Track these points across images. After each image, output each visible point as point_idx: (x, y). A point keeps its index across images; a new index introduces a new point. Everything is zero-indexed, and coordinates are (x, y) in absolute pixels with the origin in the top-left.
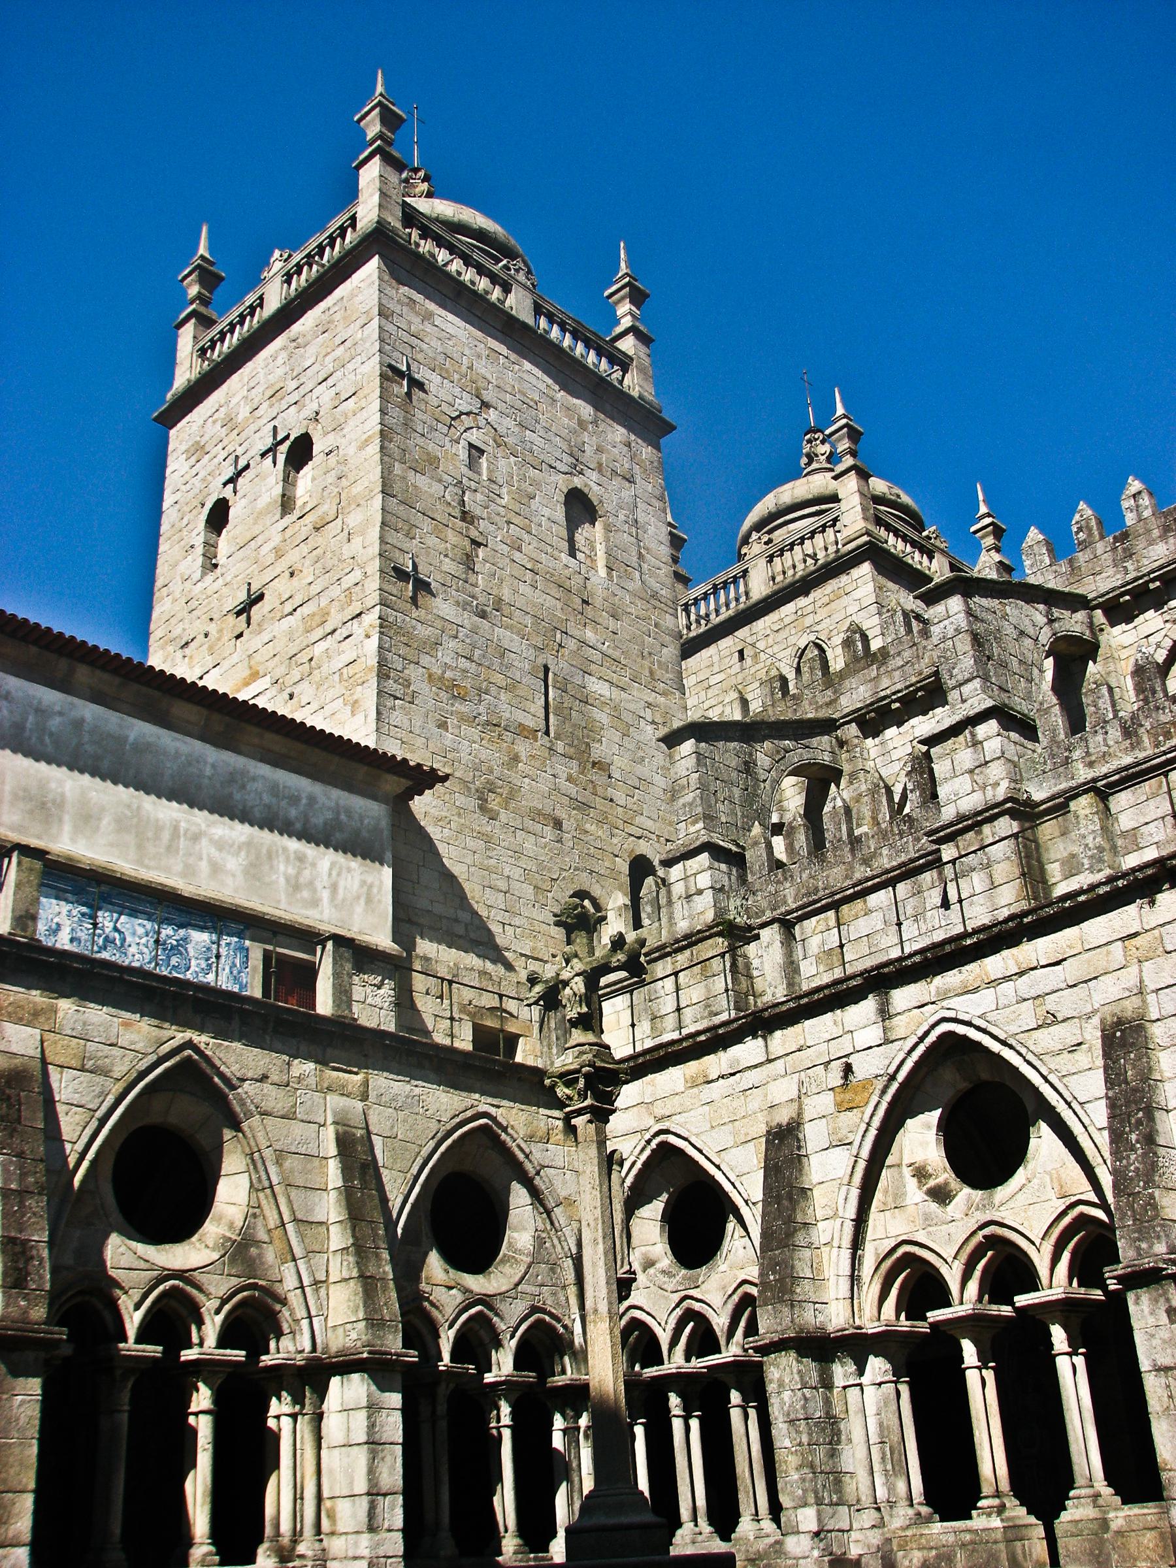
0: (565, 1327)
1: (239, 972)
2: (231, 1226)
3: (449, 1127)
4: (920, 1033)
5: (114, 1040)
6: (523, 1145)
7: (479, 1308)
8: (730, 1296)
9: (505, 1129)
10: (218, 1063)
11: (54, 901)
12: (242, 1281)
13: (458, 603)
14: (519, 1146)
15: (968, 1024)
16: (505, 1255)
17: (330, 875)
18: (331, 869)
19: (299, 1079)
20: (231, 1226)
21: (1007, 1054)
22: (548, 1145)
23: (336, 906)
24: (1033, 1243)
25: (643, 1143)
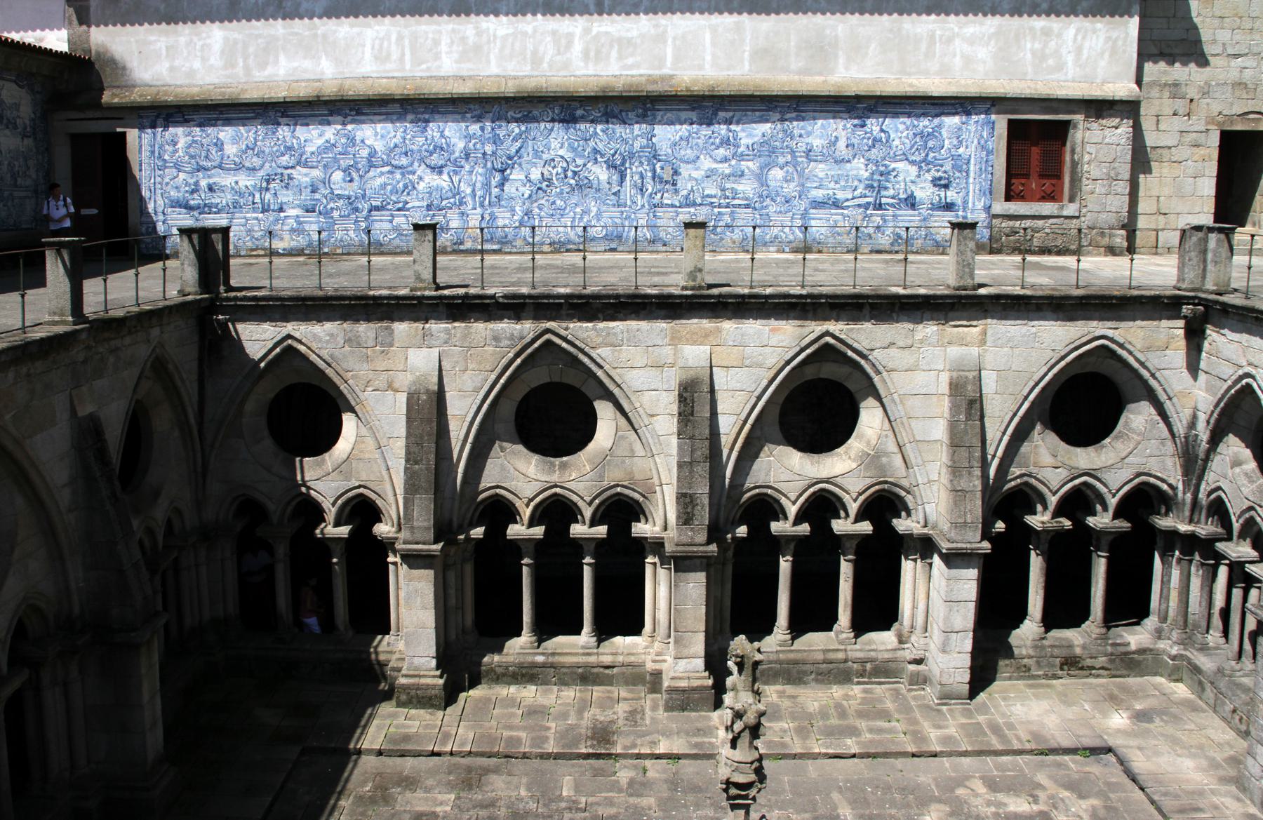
0: (1170, 486)
1: (986, 142)
2: (868, 443)
3: (1063, 353)
5: (766, 343)
9: (1121, 346)
10: (850, 341)
11: (832, 121)
12: (874, 481)
16: (1120, 432)
19: (921, 341)
20: (868, 443)
22: (1168, 352)
23: (1080, 66)
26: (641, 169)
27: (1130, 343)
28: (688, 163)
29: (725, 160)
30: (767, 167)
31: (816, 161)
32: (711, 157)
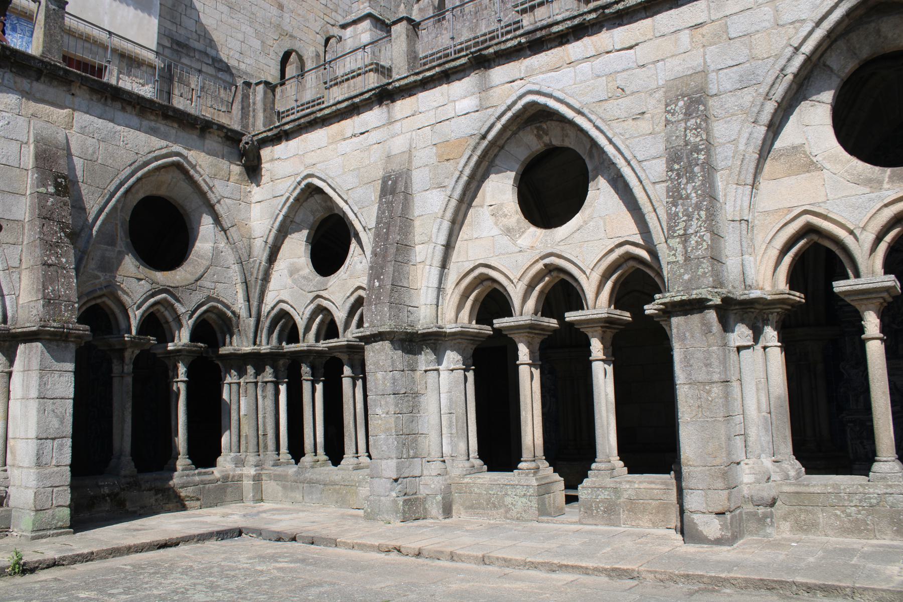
0: (234, 313)
3: (145, 159)
4: (509, 102)
6: (208, 180)
7: (164, 295)
8: (348, 297)
9: (194, 167)
14: (204, 180)
15: (550, 96)
21: (580, 120)
24: (584, 272)
25: (295, 183)
27: (200, 166)
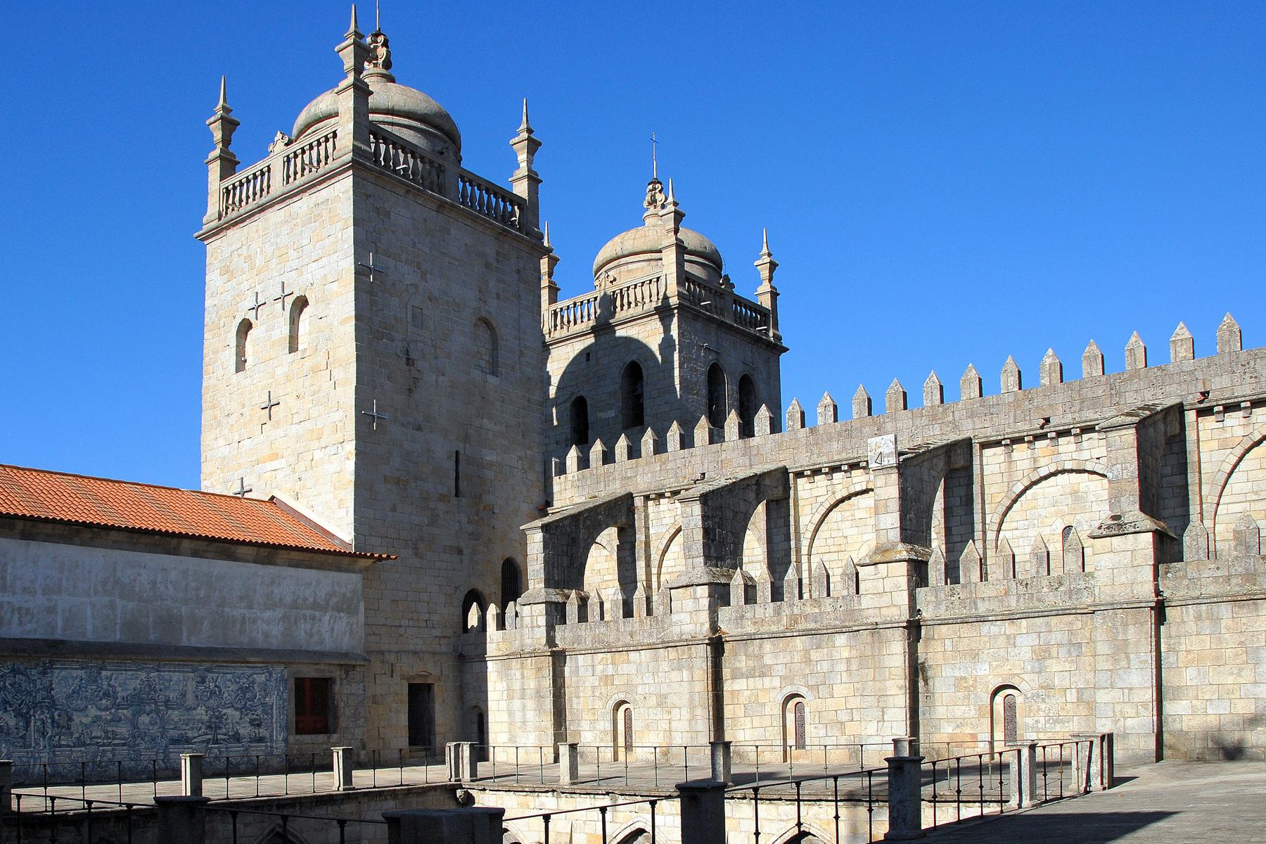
13: (403, 425)
17: (329, 624)
18: (330, 620)
26: (42, 716)
28: (81, 711)
29: (106, 709)
30: (137, 714)
31: (172, 709)
32: (96, 706)
